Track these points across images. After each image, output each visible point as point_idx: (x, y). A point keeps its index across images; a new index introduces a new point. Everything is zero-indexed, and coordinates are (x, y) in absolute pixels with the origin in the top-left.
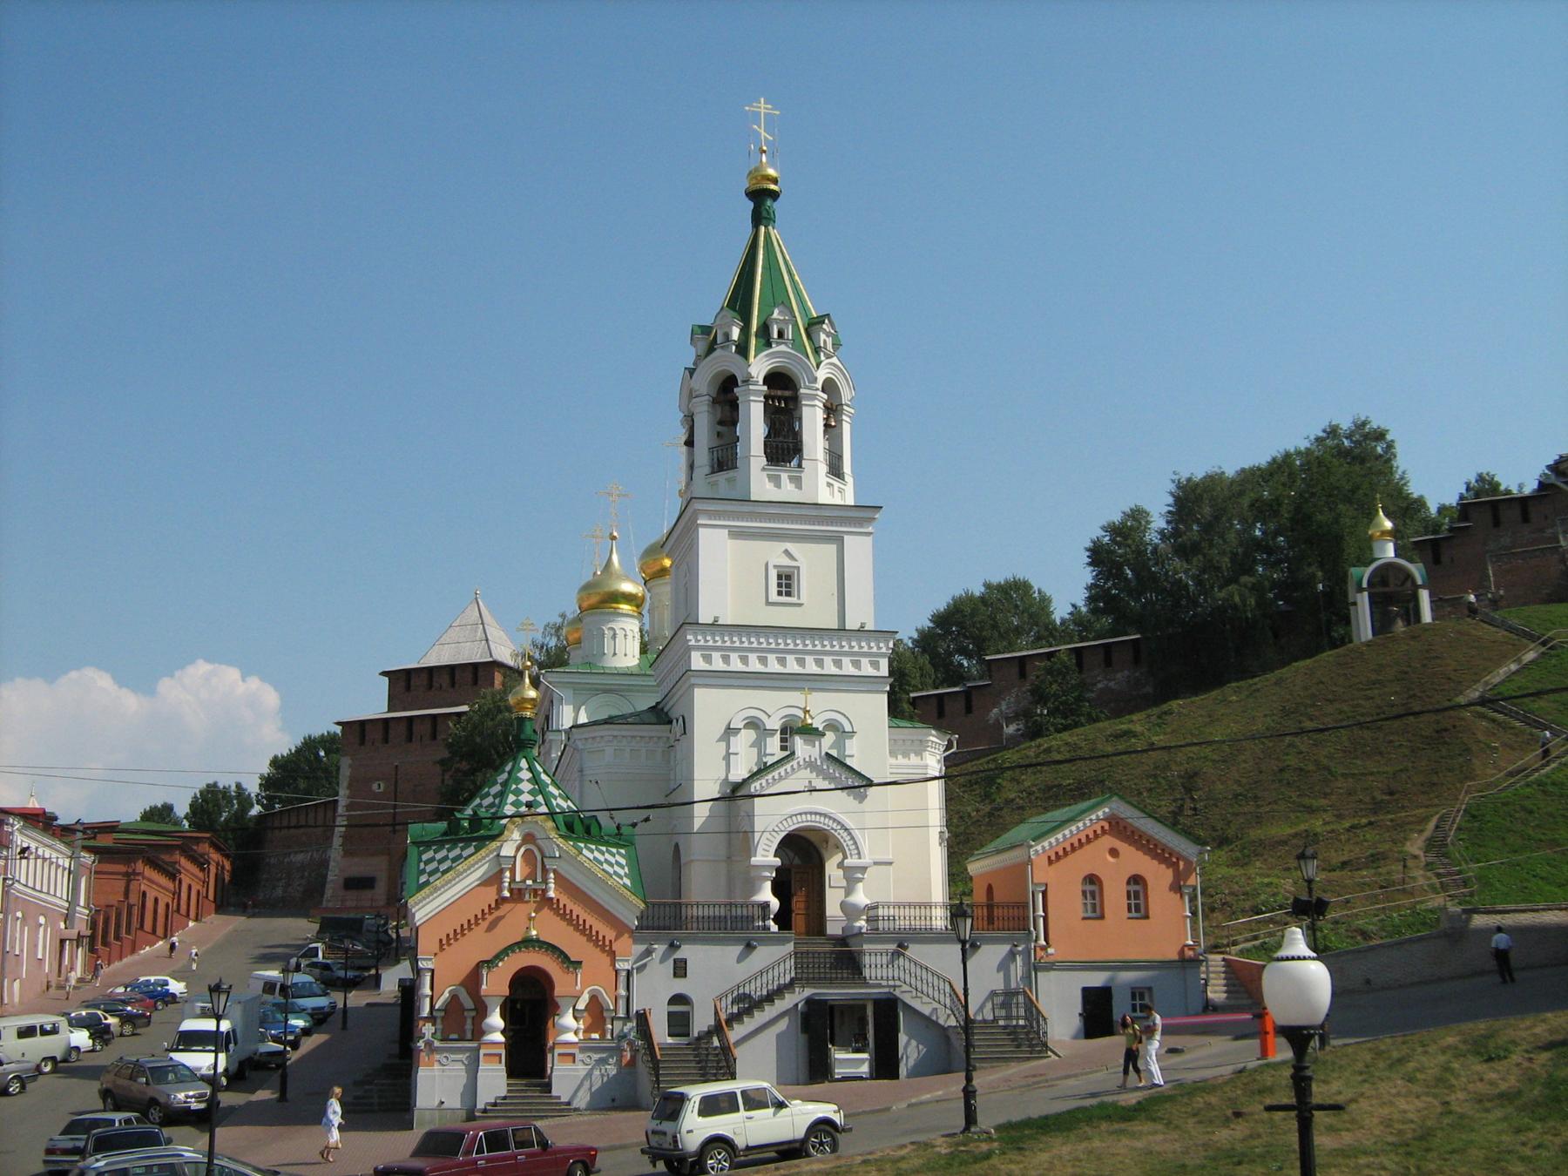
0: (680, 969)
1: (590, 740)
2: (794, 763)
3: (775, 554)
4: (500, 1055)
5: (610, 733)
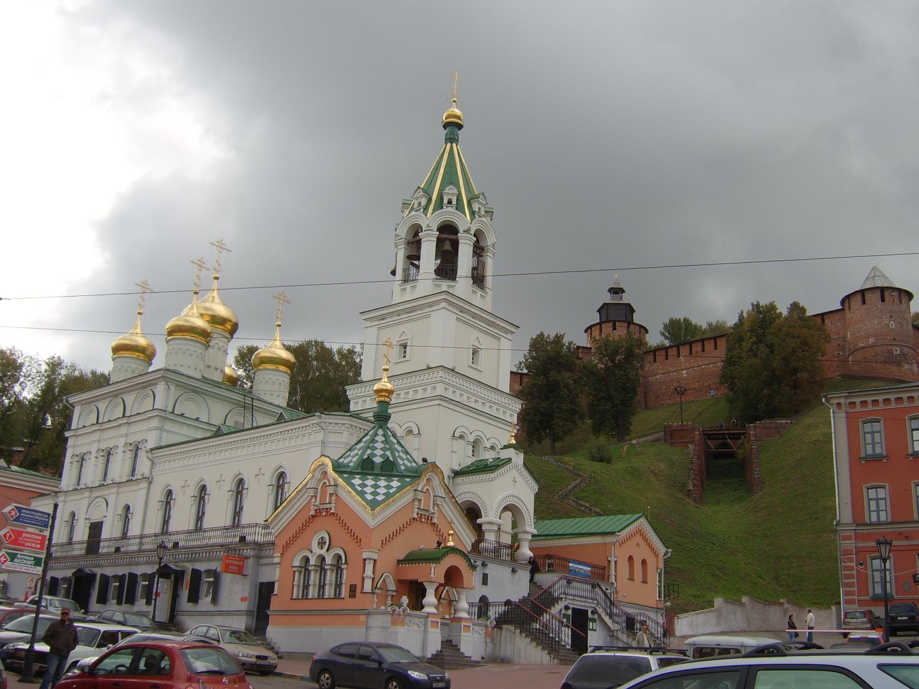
0: (485, 581)
1: (333, 425)
2: (510, 465)
3: (472, 337)
4: (438, 622)
5: (348, 422)
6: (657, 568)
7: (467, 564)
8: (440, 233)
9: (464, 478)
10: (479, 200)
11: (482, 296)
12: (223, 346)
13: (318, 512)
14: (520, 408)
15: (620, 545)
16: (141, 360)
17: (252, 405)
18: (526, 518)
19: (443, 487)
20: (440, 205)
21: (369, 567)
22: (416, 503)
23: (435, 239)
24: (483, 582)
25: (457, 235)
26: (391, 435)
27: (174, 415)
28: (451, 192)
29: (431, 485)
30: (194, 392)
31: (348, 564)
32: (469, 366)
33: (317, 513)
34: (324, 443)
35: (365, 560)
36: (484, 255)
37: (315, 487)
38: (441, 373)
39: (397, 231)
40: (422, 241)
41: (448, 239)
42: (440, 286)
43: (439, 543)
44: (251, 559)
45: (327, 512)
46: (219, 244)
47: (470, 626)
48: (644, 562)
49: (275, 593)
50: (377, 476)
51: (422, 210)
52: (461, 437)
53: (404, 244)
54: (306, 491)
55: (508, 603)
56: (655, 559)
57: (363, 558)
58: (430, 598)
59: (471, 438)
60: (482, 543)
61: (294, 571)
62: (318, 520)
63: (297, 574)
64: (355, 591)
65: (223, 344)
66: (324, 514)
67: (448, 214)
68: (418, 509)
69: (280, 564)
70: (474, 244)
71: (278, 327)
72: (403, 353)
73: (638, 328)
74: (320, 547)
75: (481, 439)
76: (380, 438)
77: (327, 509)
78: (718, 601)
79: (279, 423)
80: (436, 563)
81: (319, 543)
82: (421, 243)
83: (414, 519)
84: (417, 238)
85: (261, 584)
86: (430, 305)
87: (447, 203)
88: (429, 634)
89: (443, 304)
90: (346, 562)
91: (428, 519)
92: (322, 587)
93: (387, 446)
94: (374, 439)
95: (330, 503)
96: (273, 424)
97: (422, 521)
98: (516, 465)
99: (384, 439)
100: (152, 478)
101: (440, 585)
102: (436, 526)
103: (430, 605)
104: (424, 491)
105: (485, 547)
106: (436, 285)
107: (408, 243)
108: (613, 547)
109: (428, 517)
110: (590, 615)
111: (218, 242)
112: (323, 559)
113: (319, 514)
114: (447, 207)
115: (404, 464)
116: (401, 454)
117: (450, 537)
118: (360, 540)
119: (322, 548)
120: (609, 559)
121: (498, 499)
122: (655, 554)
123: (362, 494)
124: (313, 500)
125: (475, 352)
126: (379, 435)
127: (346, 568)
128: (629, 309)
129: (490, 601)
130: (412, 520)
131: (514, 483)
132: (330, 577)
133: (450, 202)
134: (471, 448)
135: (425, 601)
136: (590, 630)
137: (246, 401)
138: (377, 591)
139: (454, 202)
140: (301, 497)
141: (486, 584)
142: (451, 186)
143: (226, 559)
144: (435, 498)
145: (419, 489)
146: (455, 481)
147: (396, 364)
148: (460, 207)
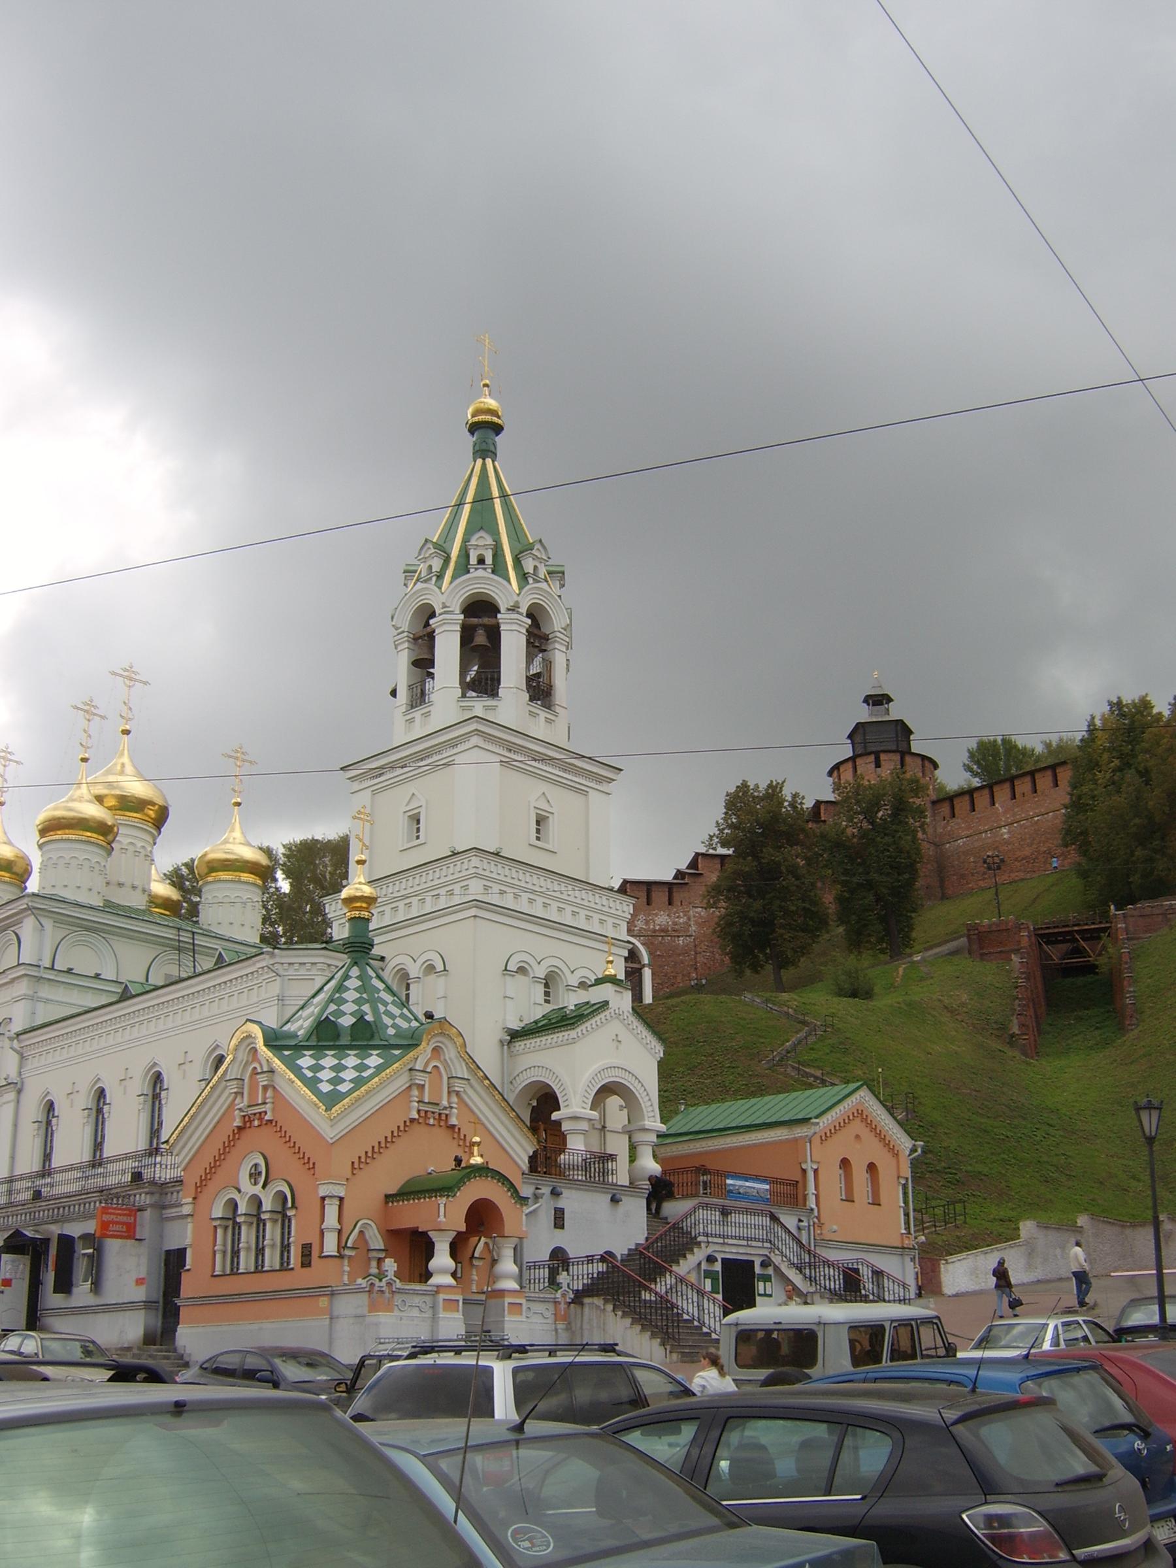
0: (559, 1220)
1: (296, 967)
2: (607, 1013)
4: (458, 1301)
5: (322, 960)
6: (898, 1177)
7: (509, 1194)
8: (465, 617)
9: (527, 1042)
10: (534, 552)
11: (548, 720)
12: (143, 847)
13: (247, 1121)
14: (632, 912)
15: (822, 1140)
16: (5, 882)
17: (194, 944)
18: (643, 1105)
19: (464, 1060)
20: (464, 567)
21: (332, 1211)
22: (415, 1092)
23: (458, 628)
24: (555, 1224)
25: (496, 617)
26: (374, 975)
27: (56, 973)
28: (481, 542)
29: (442, 1059)
30: (87, 929)
31: (296, 1208)
32: (530, 845)
33: (245, 1123)
34: (282, 1000)
35: (323, 1199)
36: (550, 647)
37: (239, 1077)
38: (475, 861)
39: (394, 620)
40: (437, 632)
41: (480, 625)
42: (470, 708)
43: (458, 1161)
44: (149, 1210)
45: (261, 1119)
46: (126, 674)
47: (521, 1304)
48: (872, 1167)
49: (187, 1267)
50: (341, 1049)
51: (434, 579)
52: (522, 970)
53: (408, 641)
54: (226, 1087)
55: (607, 1257)
56: (894, 1160)
58: (442, 1259)
59: (541, 971)
60: (562, 1156)
62: (247, 1135)
63: (220, 1231)
64: (310, 1255)
65: (143, 844)
66: (256, 1123)
67: (481, 582)
68: (418, 1102)
69: (192, 1215)
70: (527, 631)
71: (236, 807)
72: (415, 831)
73: (919, 761)
74: (253, 1180)
75: (560, 973)
76: (353, 983)
77: (260, 1113)
78: (1027, 1227)
79: (219, 968)
80: (448, 1196)
81: (251, 1175)
82: (434, 637)
83: (412, 1120)
84: (429, 629)
85: (168, 1252)
86: (453, 743)
87: (476, 563)
88: (441, 1323)
89: (475, 740)
90: (294, 1206)
91: (440, 1118)
92: (260, 1251)
93: (364, 996)
94: (342, 984)
95: (265, 1103)
96: (209, 971)
97: (429, 1124)
98: (617, 1012)
99: (361, 983)
100: (22, 1083)
101: (459, 1233)
102: (457, 1130)
103: (443, 1271)
104: (429, 1070)
105: (576, 1163)
106: (464, 708)
107: (415, 639)
108: (808, 1144)
109: (440, 1114)
110: (758, 1270)
111: (126, 670)
112: (257, 1202)
113: (248, 1125)
114: (476, 569)
115: (394, 1026)
116: (391, 1008)
117: (476, 1148)
118: (314, 1164)
119: (256, 1184)
120: (804, 1166)
121: (587, 1075)
122: (895, 1153)
123: (312, 1083)
124: (238, 1100)
125: (540, 821)
126: (351, 977)
127: (294, 1215)
128: (902, 730)
129: (571, 1256)
130: (408, 1124)
131: (615, 1043)
132: (272, 1232)
133: (481, 561)
134: (541, 989)
135: (433, 1264)
136: (760, 1295)
137: (181, 939)
138: (347, 1252)
139: (489, 560)
140: (219, 1096)
141: (562, 1227)
142: (482, 533)
143: (103, 1213)
144: (452, 1081)
145: (417, 1068)
146: (512, 1049)
147: (405, 852)
148: (498, 568)
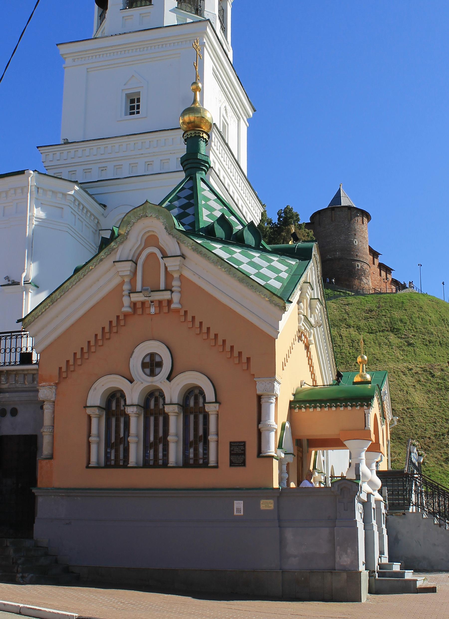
31: (220, 403)
57: (259, 392)
61: (89, 418)
64: (244, 454)
66: (153, 310)
77: (160, 302)
113: (139, 311)
118: (248, 359)
119: (152, 374)
